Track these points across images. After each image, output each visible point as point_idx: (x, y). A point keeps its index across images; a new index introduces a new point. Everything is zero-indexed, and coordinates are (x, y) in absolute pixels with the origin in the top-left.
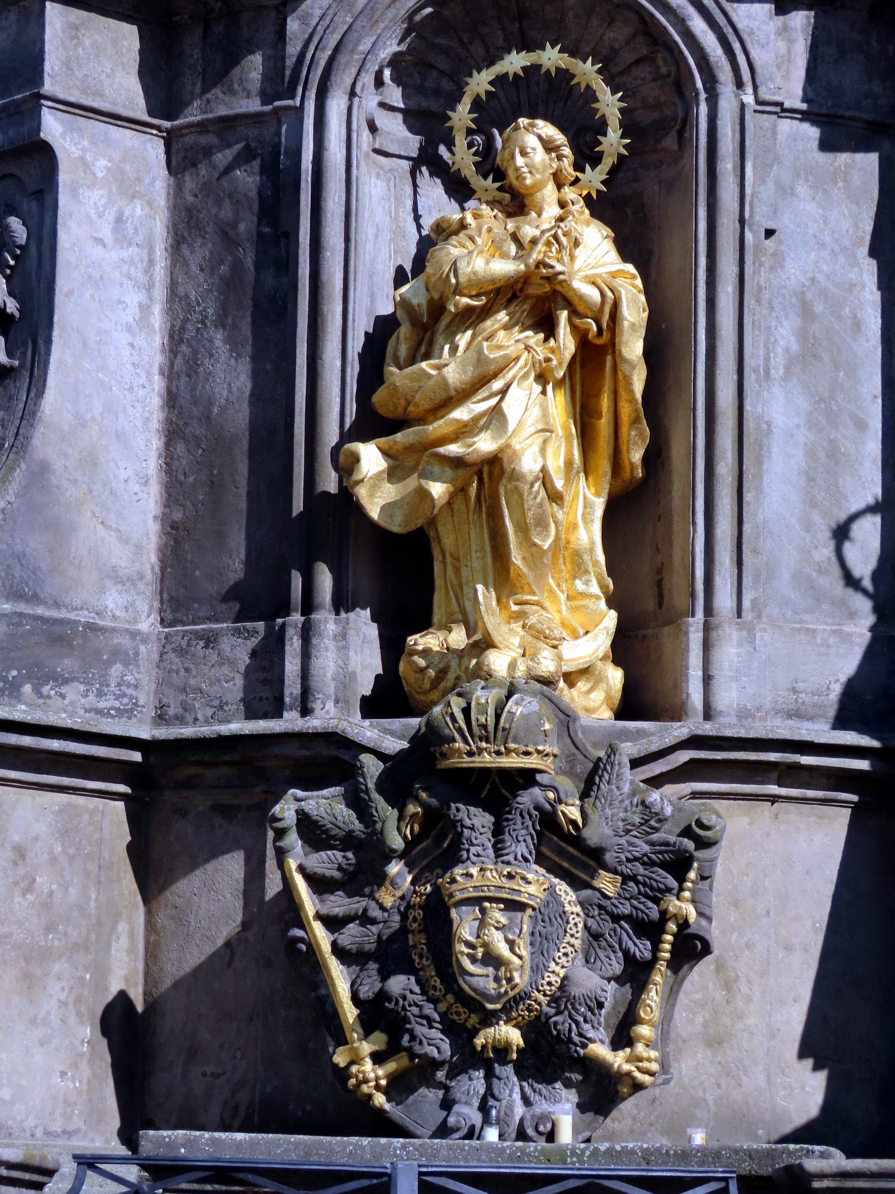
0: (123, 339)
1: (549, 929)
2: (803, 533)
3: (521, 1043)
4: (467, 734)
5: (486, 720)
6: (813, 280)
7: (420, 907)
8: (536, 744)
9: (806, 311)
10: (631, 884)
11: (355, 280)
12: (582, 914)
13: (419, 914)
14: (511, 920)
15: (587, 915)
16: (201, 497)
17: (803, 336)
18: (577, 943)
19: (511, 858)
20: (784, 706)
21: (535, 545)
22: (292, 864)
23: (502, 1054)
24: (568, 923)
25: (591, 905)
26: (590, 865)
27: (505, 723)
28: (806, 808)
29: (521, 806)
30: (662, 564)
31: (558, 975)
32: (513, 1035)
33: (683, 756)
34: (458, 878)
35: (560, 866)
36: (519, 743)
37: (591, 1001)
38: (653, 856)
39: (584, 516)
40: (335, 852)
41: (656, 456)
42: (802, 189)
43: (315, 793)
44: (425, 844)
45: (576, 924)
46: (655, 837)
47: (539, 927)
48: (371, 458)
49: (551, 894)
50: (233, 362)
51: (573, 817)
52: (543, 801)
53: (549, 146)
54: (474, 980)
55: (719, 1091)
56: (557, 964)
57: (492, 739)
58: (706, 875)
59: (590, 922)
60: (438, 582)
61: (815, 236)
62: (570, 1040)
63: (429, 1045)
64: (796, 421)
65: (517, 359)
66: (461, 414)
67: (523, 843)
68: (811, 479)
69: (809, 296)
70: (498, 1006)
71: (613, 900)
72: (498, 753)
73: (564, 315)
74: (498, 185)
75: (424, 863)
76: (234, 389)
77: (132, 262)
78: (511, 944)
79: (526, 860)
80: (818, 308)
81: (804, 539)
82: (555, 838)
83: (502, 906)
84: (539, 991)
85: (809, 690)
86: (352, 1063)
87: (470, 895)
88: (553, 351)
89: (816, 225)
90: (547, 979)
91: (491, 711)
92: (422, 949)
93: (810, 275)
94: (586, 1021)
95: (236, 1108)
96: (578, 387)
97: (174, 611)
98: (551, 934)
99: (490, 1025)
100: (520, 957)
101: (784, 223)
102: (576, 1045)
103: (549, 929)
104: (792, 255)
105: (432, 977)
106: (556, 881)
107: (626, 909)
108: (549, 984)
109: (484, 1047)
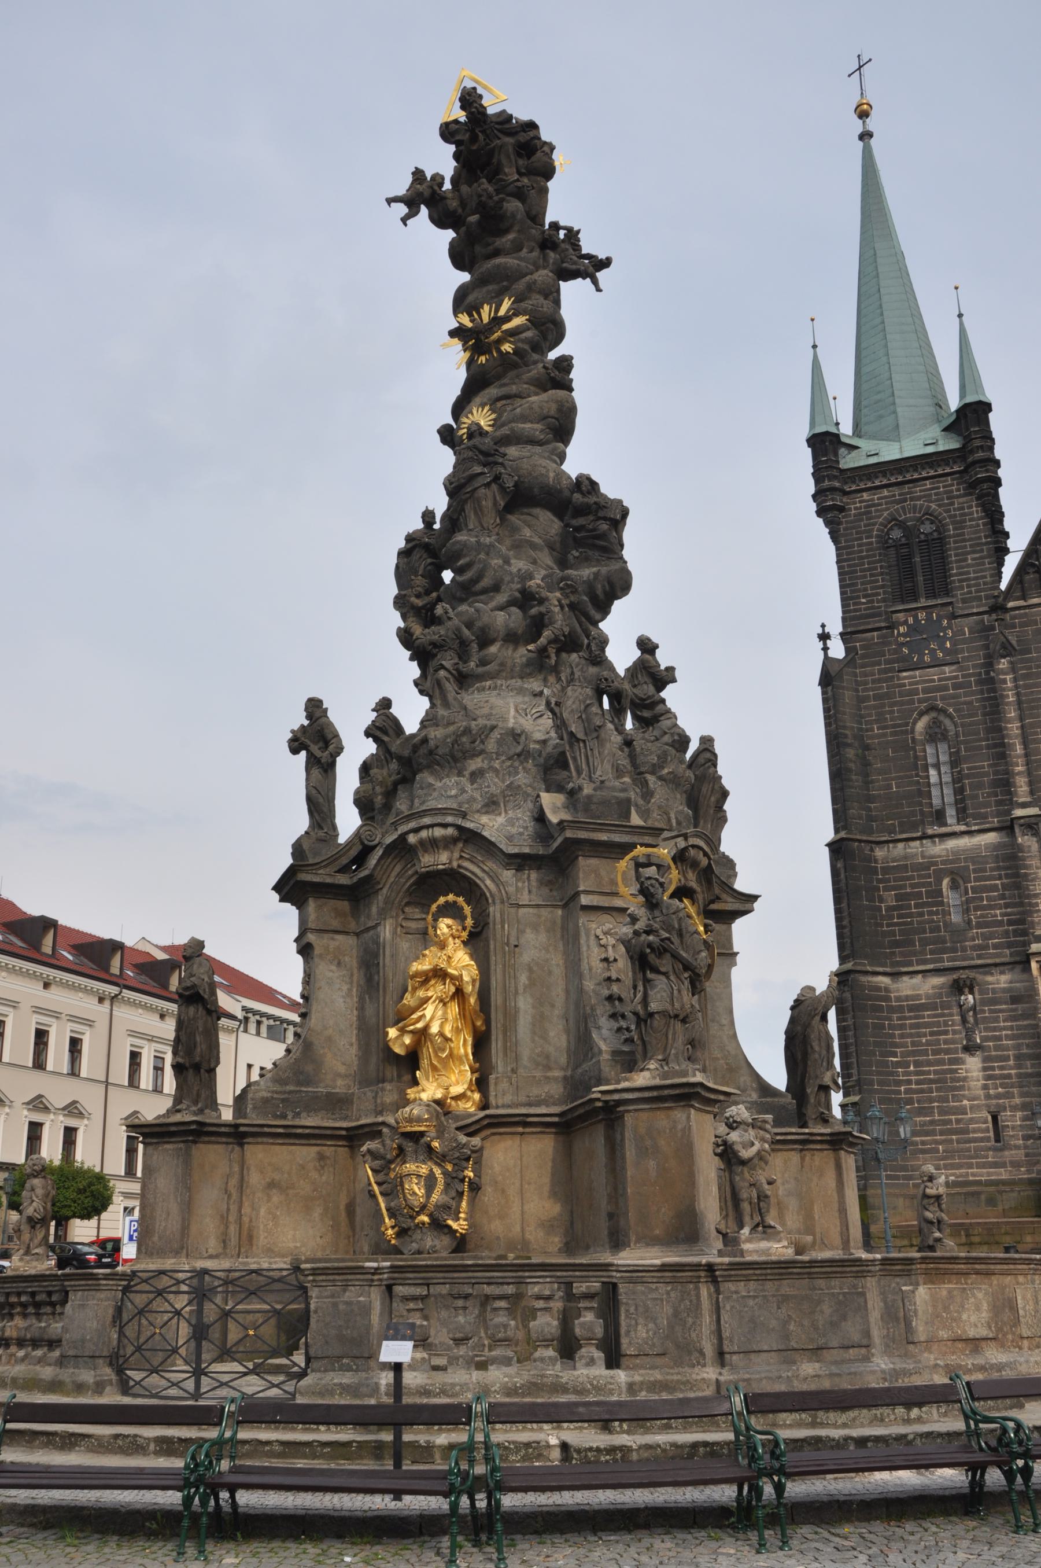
0: (342, 1000)
9: (530, 970)
17: (529, 978)
28: (534, 1136)
32: (426, 1219)
33: (485, 1122)
39: (463, 1045)
48: (392, 1033)
53: (449, 927)
66: (414, 1016)
77: (344, 976)
80: (535, 968)
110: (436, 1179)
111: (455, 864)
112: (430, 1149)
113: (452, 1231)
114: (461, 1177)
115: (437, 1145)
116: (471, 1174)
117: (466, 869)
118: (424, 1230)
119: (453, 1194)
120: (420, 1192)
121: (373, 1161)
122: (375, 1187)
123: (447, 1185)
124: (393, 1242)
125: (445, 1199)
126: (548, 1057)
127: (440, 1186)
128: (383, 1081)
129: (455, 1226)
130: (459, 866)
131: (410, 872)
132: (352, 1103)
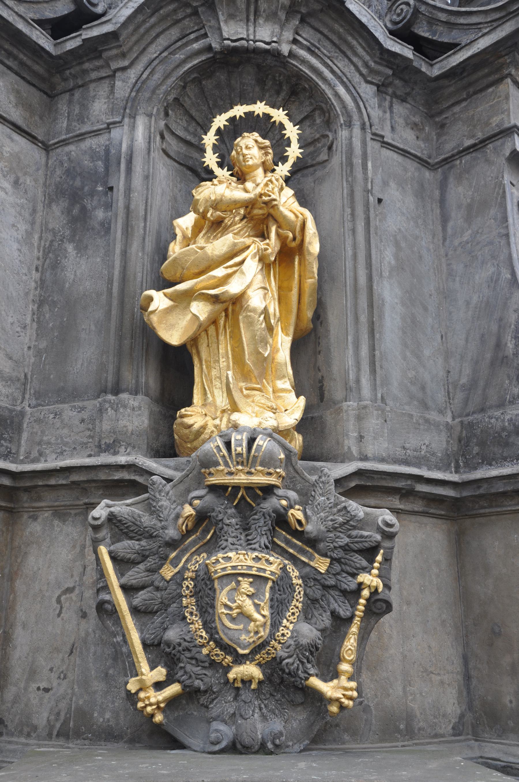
0: (15, 246)
1: (284, 596)
2: (402, 361)
3: (261, 676)
4: (228, 460)
5: (242, 449)
6: (400, 229)
7: (192, 579)
8: (275, 468)
9: (397, 244)
10: (337, 564)
11: (151, 210)
12: (302, 585)
13: (190, 584)
14: (257, 590)
15: (306, 585)
16: (56, 334)
17: (396, 257)
18: (300, 605)
19: (257, 546)
21: (260, 353)
22: (103, 550)
23: (247, 685)
24: (295, 591)
25: (309, 579)
26: (308, 551)
27: (255, 452)
28: (413, 518)
29: (264, 510)
30: (323, 377)
31: (288, 629)
34: (220, 560)
35: (287, 552)
36: (264, 467)
37: (313, 647)
38: (352, 545)
40: (133, 541)
41: (319, 317)
42: (392, 184)
43: (120, 502)
44: (193, 537)
45: (299, 593)
46: (354, 533)
47: (277, 595)
48: (160, 300)
49: (284, 571)
50: (78, 259)
51: (299, 518)
52: (279, 507)
54: (230, 633)
55: (376, 699)
56: (288, 620)
57: (245, 464)
58: (389, 558)
59: (308, 590)
60: (197, 379)
62: (296, 675)
63: (197, 679)
64: (396, 301)
65: (248, 247)
67: (265, 536)
68: (404, 333)
69: (398, 237)
70: (246, 651)
71: (324, 576)
72: (250, 473)
73: (273, 229)
74: (230, 172)
75: (194, 549)
76: (78, 273)
77: (22, 207)
78: (257, 606)
79: (267, 547)
80: (403, 245)
81: (403, 364)
82: (284, 533)
83: (251, 580)
84: (276, 640)
85: (411, 448)
86: (141, 689)
87: (229, 572)
88: (268, 244)
90: (282, 632)
91: (245, 444)
92: (192, 608)
93: (398, 227)
94: (309, 662)
95: (58, 714)
96: (277, 278)
97: (36, 399)
98: (285, 600)
99: (240, 663)
100: (264, 616)
101: (385, 198)
102: (301, 679)
103: (284, 596)
104: (389, 215)
105: (200, 629)
106: (286, 562)
107: (331, 582)
108: (283, 635)
109: (235, 680)
110: (292, 586)
111: (285, 49)
112: (281, 520)
113: (317, 698)
114: (353, 586)
115: (300, 515)
116: (377, 582)
117: (304, 61)
118: (245, 695)
119: (326, 621)
120: (261, 616)
121: (115, 540)
122: (120, 598)
123: (311, 604)
124: (159, 718)
125: (309, 632)
126: (423, 388)
127: (297, 603)
128: (116, 391)
129: (327, 688)
130: (291, 54)
131: (196, 46)
132: (19, 430)
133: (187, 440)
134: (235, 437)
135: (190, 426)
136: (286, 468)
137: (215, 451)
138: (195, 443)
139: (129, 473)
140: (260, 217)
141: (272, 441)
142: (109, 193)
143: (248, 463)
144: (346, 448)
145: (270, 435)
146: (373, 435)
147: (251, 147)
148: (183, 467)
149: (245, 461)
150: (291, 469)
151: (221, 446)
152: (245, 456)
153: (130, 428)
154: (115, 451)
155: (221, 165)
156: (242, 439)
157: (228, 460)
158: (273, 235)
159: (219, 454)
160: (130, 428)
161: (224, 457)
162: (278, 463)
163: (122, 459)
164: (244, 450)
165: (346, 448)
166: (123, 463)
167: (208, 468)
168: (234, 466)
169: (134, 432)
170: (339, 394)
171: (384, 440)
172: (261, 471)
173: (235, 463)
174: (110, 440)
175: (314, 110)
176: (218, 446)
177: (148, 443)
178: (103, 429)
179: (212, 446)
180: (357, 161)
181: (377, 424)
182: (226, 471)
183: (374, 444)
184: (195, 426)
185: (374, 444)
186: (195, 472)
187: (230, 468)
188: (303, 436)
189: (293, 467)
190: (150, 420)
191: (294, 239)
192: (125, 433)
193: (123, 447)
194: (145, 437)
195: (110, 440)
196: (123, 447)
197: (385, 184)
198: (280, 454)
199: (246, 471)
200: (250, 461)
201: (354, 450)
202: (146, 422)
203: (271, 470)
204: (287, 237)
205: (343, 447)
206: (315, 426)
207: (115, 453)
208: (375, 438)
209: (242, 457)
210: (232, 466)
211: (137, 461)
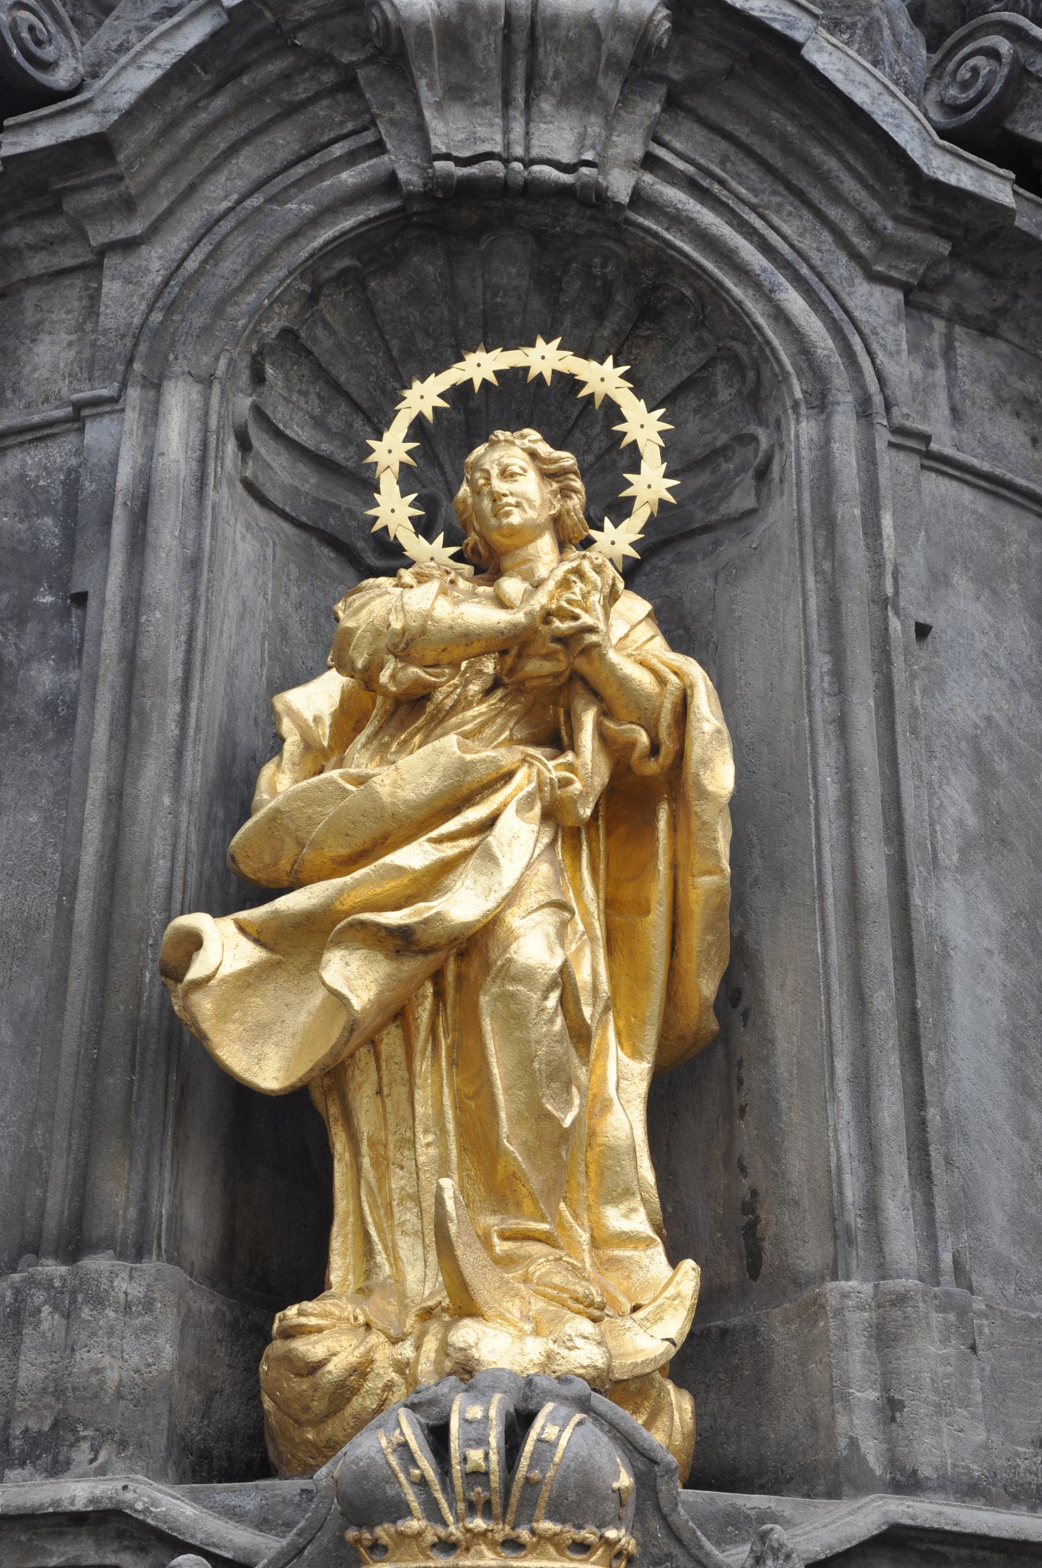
2: (1017, 1141)
4: (439, 1495)
6: (989, 719)
8: (602, 1525)
9: (982, 765)
11: (203, 663)
17: (982, 804)
20: (1030, 1477)
21: (549, 1116)
27: (531, 1467)
30: (754, 1193)
36: (563, 1522)
41: (736, 995)
42: (961, 581)
48: (224, 947)
57: (497, 1510)
60: (342, 1203)
61: (986, 655)
64: (986, 943)
65: (509, 776)
68: (1019, 1047)
69: (985, 744)
73: (588, 719)
74: (453, 550)
80: (1002, 766)
81: (1019, 1152)
88: (570, 767)
89: (985, 640)
91: (495, 1437)
93: (983, 710)
101: (938, 620)
104: (954, 675)
111: (620, 184)
117: (677, 220)
128: (74, 1246)
130: (639, 199)
131: (349, 177)
133: (304, 1417)
134: (462, 1412)
135: (315, 1368)
136: (639, 1527)
137: (394, 1461)
138: (332, 1428)
139: (99, 1543)
140: (546, 683)
141: (589, 1424)
142: (75, 612)
143: (505, 1506)
144: (843, 1442)
145: (583, 1404)
146: (933, 1397)
147: (517, 473)
148: (288, 1512)
149: (497, 1500)
150: (655, 1525)
151: (414, 1445)
152: (495, 1480)
153: (112, 1376)
154: (55, 1461)
155: (424, 528)
156: (486, 1417)
157: (439, 1495)
158: (587, 737)
159: (408, 1474)
160: (112, 1376)
161: (422, 1483)
162: (611, 1507)
163: (77, 1492)
164: (494, 1457)
165: (843, 1442)
166: (79, 1506)
167: (368, 1522)
168: (458, 1519)
169: (125, 1391)
170: (810, 1253)
171: (973, 1416)
172: (553, 1539)
173: (461, 1506)
174: (42, 1419)
175: (709, 364)
176: (405, 1445)
177: (172, 1429)
178: (22, 1382)
179: (384, 1443)
180: (849, 512)
181: (945, 1360)
182: (430, 1538)
183: (937, 1431)
184: (330, 1367)
185: (937, 1431)
186: (324, 1539)
187: (445, 1524)
188: (695, 1396)
189: (664, 1518)
190: (181, 1346)
191: (655, 749)
192: (96, 1395)
193: (85, 1446)
194: (162, 1408)
195: (42, 1419)
196: (85, 1446)
197: (939, 579)
198: (617, 1475)
199: (499, 1537)
200: (514, 1500)
201: (872, 1450)
202: (169, 1351)
203: (588, 1534)
204: (632, 745)
205: (831, 1438)
206: (735, 1361)
207: (57, 1469)
208: (939, 1410)
209: (487, 1485)
210: (450, 1519)
211: (129, 1496)
